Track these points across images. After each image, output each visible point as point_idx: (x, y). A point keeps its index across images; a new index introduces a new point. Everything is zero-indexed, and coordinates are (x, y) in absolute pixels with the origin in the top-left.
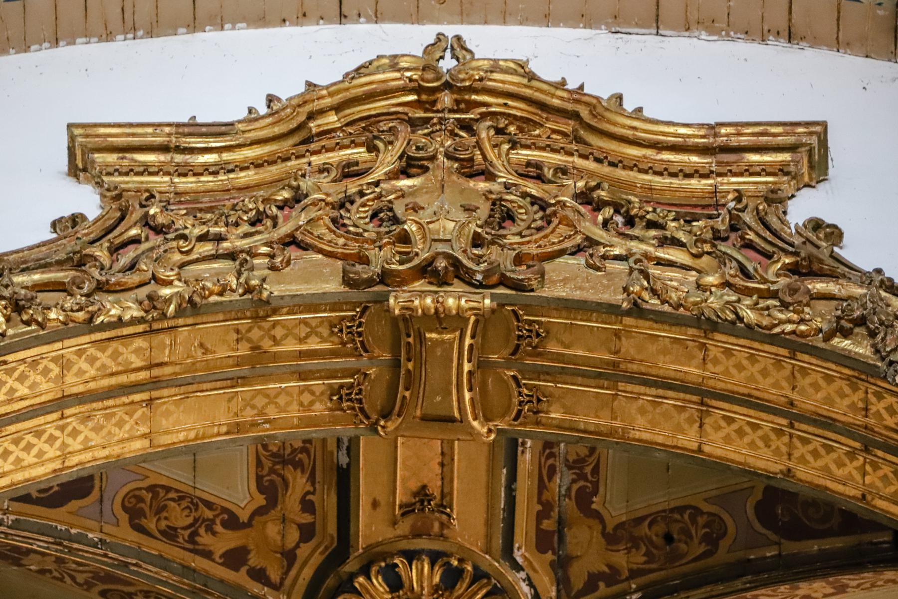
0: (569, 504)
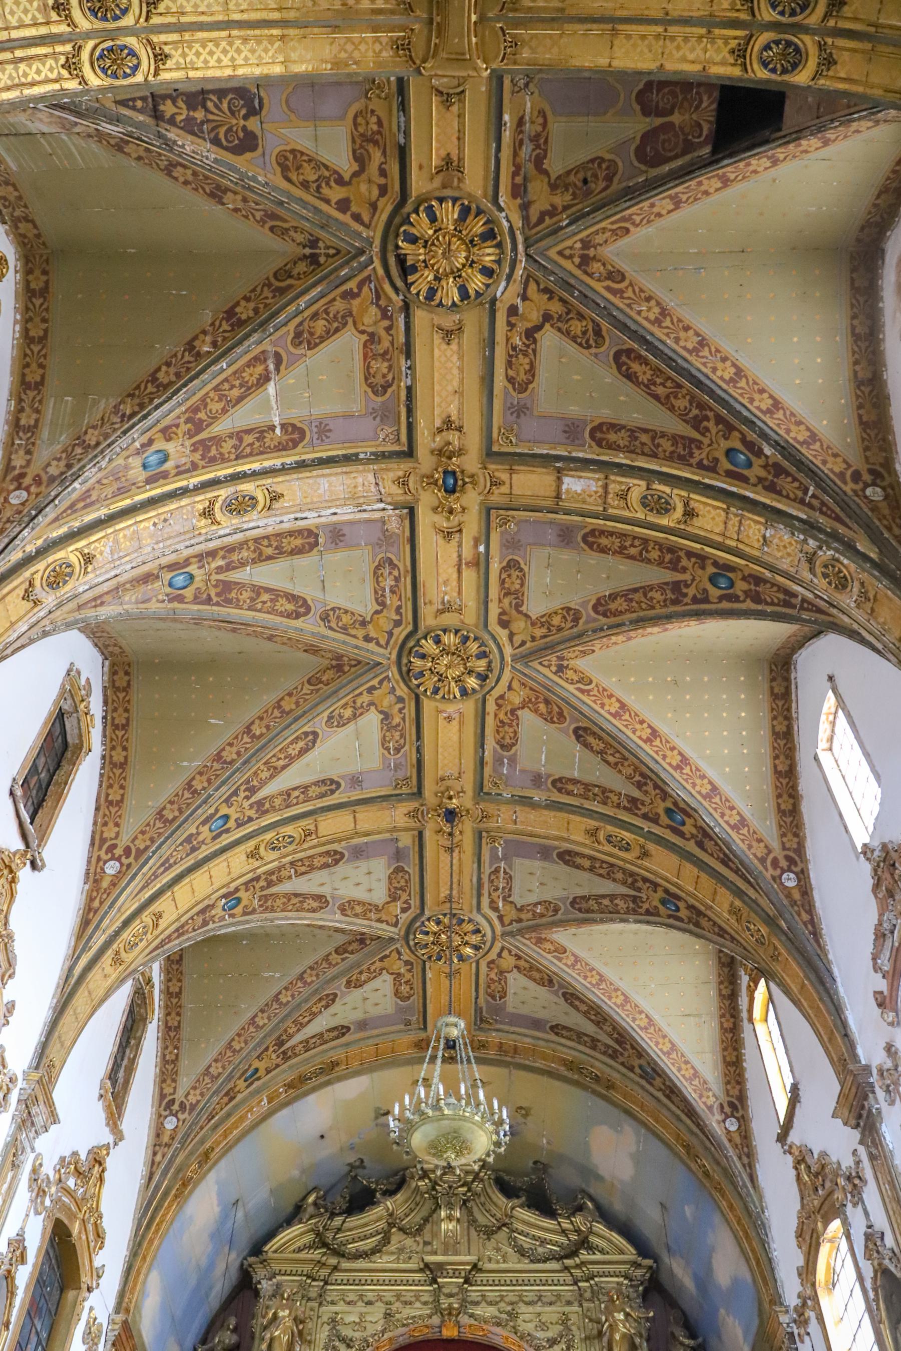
0: (530, 166)
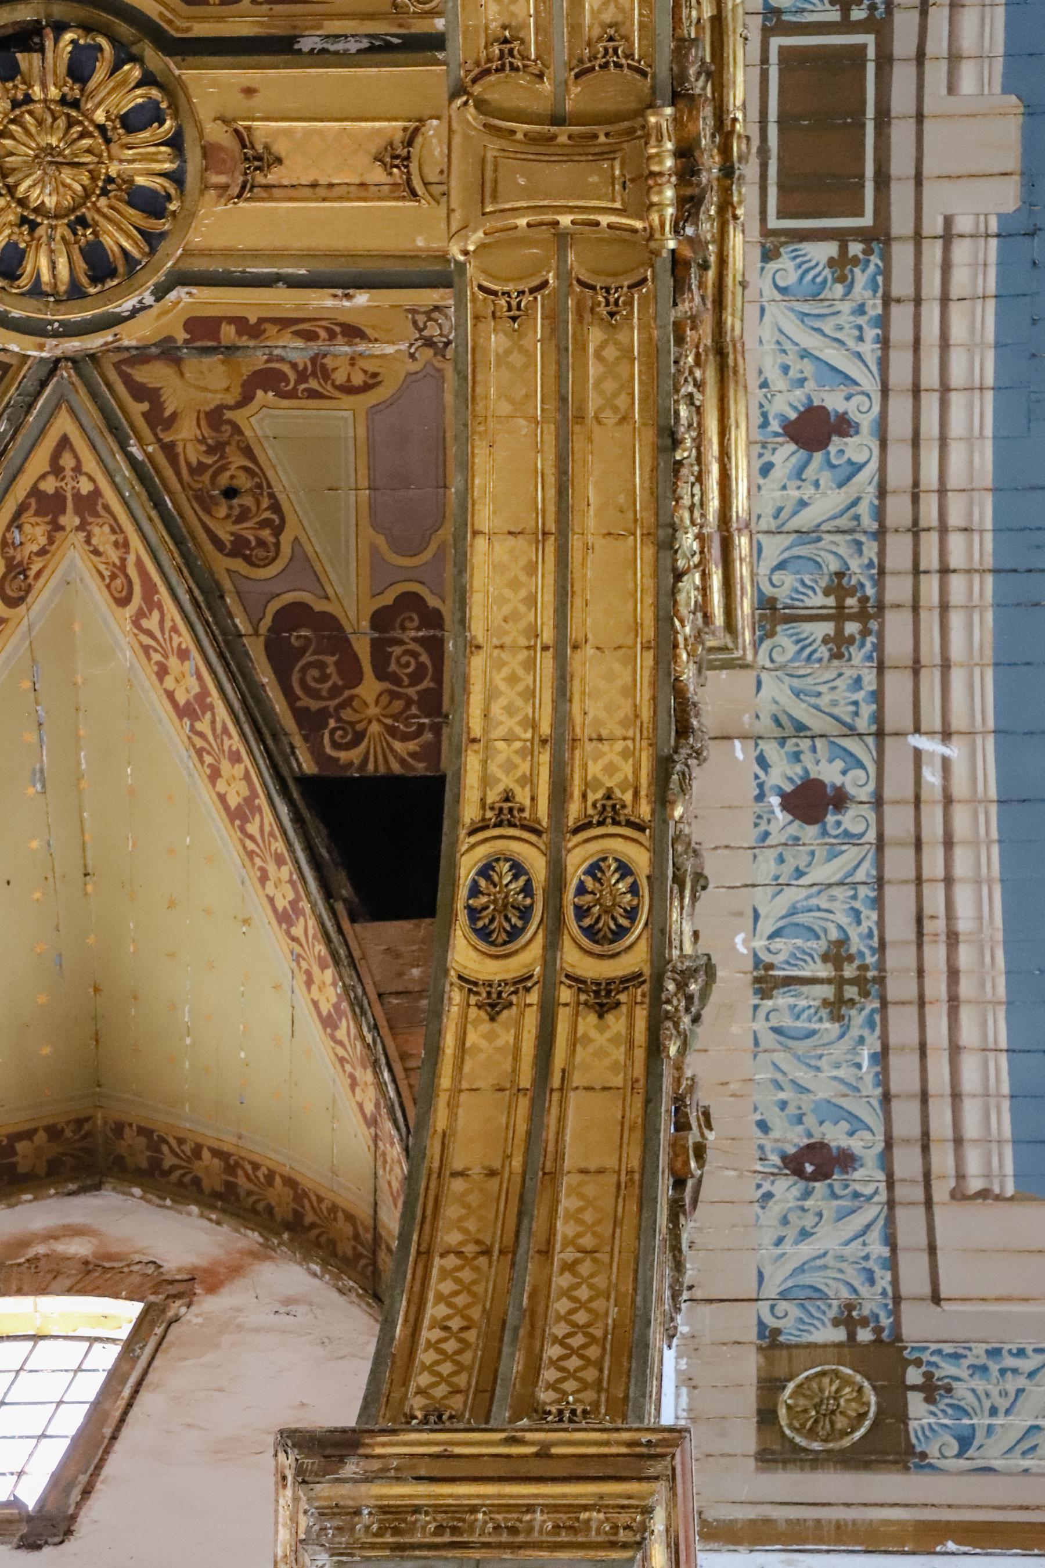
0: (258, 360)
